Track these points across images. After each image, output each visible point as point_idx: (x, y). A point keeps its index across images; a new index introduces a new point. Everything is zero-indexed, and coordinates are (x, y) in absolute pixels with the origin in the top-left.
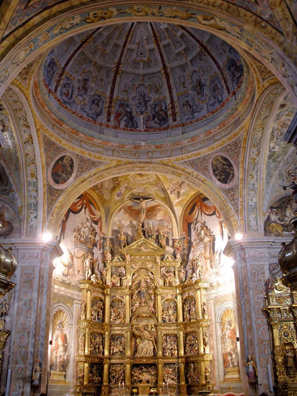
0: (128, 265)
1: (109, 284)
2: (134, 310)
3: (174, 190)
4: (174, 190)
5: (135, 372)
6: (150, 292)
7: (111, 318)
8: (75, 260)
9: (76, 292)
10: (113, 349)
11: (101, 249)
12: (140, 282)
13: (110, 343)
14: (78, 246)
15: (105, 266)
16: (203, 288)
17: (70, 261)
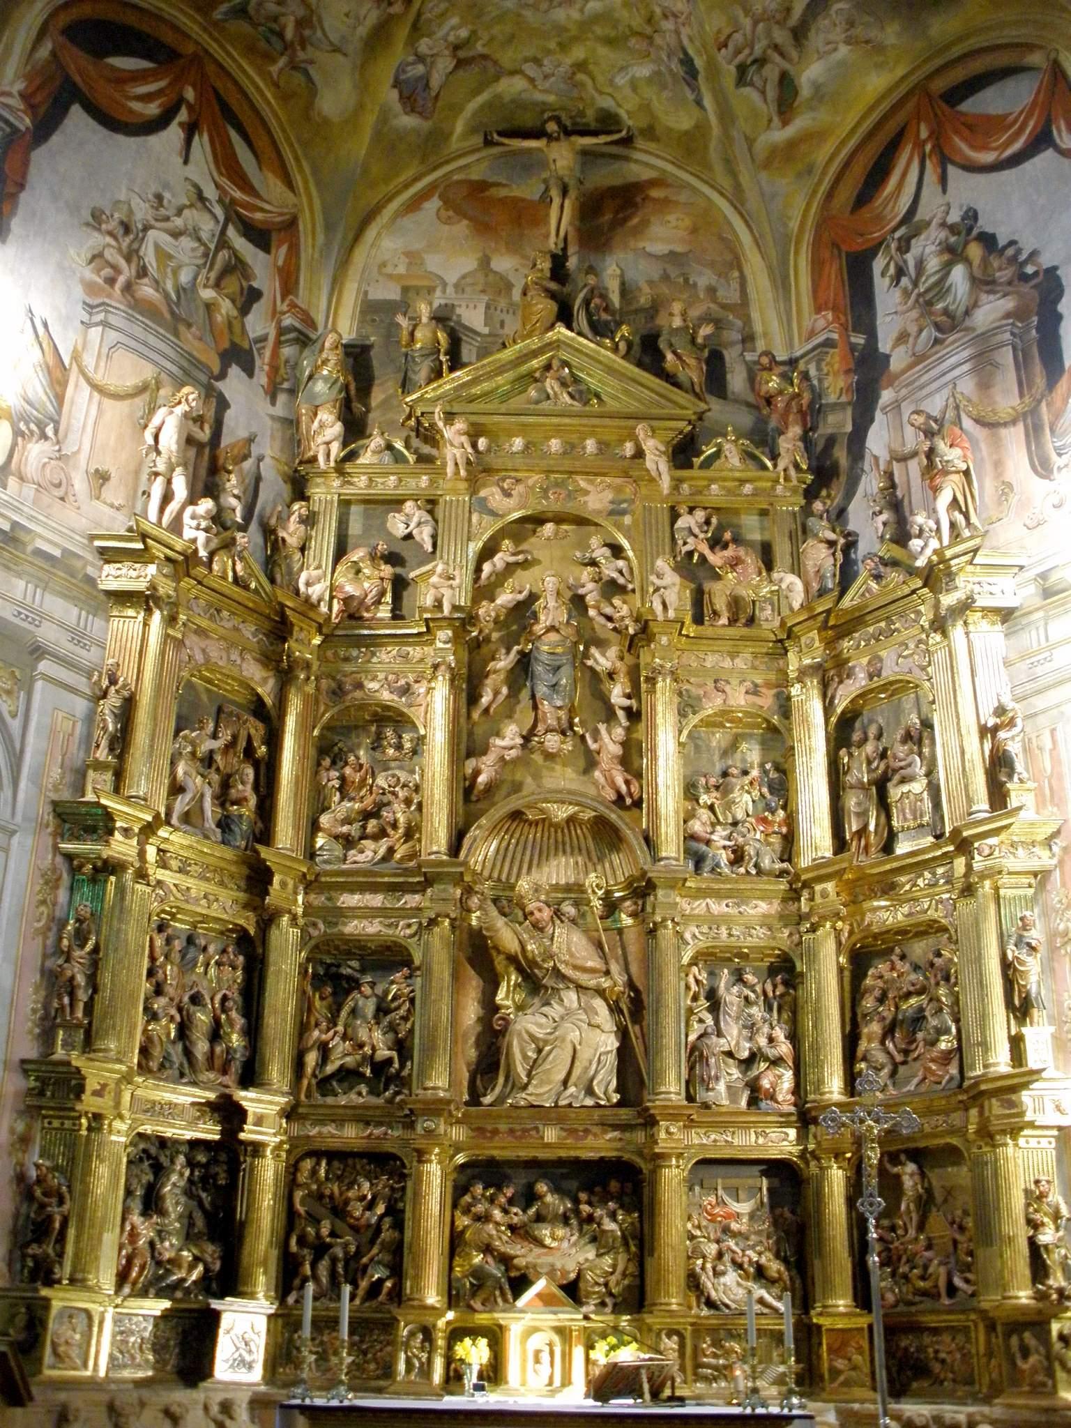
0: (455, 491)
1: (316, 591)
2: (482, 779)
3: (761, 62)
4: (761, 62)
5: (485, 1218)
6: (603, 660)
7: (315, 827)
8: (80, 397)
9: (69, 612)
10: (325, 1051)
11: (282, 398)
12: (533, 597)
13: (305, 1006)
14: (112, 319)
15: (299, 488)
16: (987, 611)
17: (38, 389)
